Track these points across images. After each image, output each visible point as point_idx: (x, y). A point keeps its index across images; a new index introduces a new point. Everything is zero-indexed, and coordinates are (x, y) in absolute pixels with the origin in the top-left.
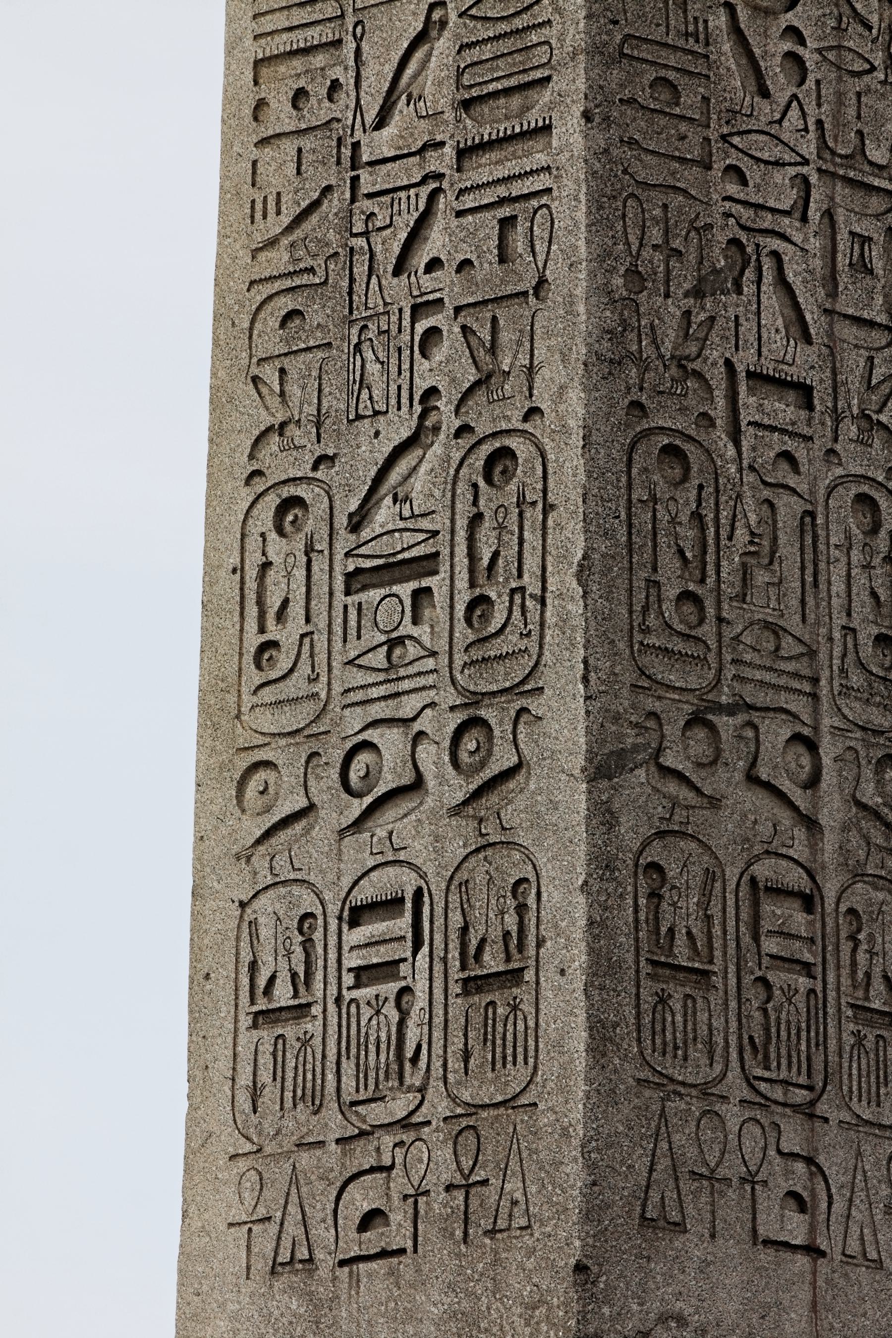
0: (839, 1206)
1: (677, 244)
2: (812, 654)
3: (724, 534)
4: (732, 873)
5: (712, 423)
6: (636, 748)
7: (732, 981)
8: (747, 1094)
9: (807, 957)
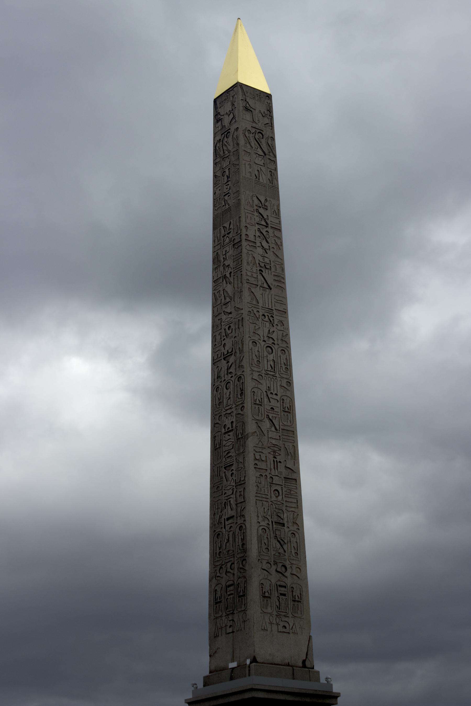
0: (236, 624)
1: (219, 507)
2: (234, 551)
3: (224, 541)
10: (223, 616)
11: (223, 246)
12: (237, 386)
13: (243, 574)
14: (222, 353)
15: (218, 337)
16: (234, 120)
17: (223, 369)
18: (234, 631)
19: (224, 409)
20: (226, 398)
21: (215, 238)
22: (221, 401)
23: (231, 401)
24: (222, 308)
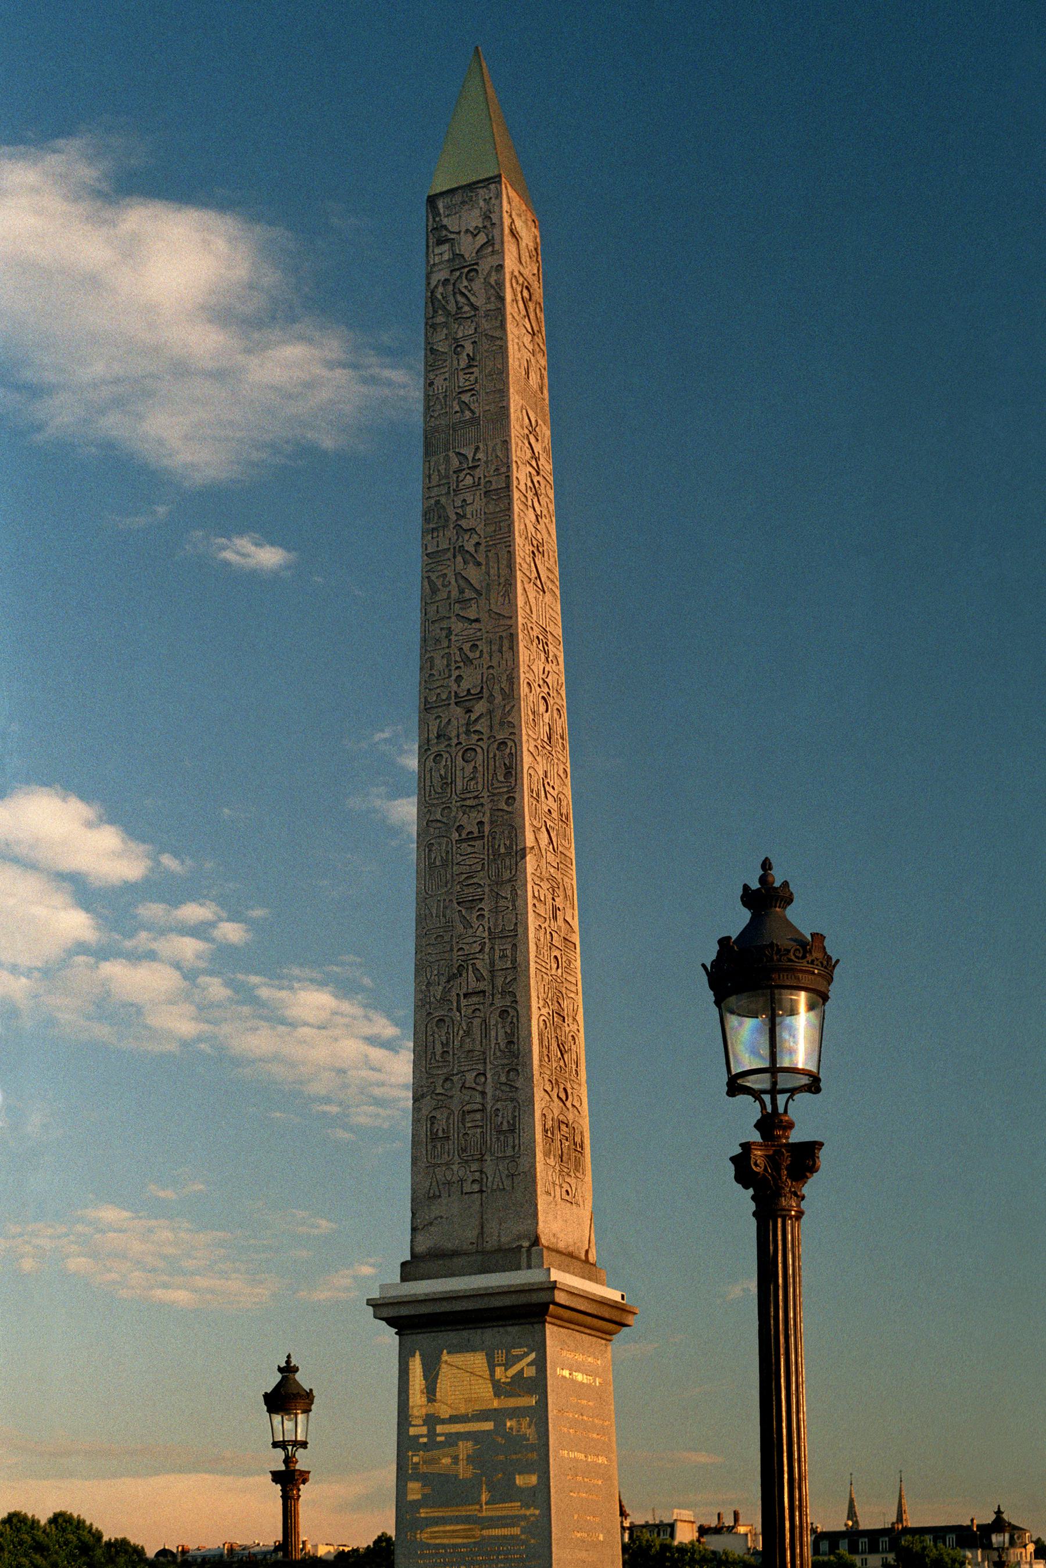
0: (490, 1179)
2: (484, 1053)
3: (455, 1034)
4: (456, 1113)
5: (452, 1009)
6: (427, 1092)
7: (456, 1136)
8: (460, 1161)
9: (481, 1124)
10: (453, 1164)
11: (454, 490)
12: (495, 759)
13: (510, 1094)
14: (450, 692)
15: (440, 663)
16: (490, 249)
17: (454, 722)
18: (484, 1189)
19: (456, 797)
20: (464, 778)
21: (431, 472)
22: (450, 780)
23: (477, 783)
24: (450, 609)
